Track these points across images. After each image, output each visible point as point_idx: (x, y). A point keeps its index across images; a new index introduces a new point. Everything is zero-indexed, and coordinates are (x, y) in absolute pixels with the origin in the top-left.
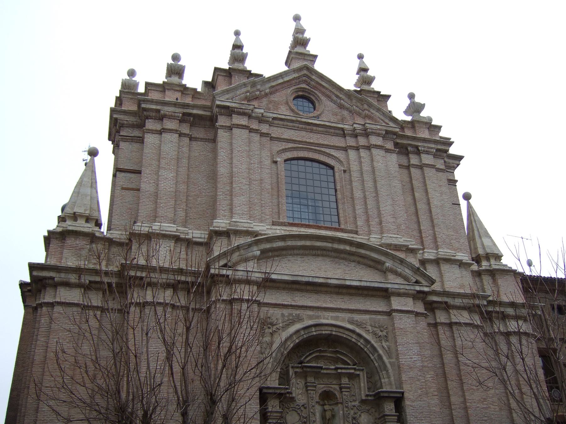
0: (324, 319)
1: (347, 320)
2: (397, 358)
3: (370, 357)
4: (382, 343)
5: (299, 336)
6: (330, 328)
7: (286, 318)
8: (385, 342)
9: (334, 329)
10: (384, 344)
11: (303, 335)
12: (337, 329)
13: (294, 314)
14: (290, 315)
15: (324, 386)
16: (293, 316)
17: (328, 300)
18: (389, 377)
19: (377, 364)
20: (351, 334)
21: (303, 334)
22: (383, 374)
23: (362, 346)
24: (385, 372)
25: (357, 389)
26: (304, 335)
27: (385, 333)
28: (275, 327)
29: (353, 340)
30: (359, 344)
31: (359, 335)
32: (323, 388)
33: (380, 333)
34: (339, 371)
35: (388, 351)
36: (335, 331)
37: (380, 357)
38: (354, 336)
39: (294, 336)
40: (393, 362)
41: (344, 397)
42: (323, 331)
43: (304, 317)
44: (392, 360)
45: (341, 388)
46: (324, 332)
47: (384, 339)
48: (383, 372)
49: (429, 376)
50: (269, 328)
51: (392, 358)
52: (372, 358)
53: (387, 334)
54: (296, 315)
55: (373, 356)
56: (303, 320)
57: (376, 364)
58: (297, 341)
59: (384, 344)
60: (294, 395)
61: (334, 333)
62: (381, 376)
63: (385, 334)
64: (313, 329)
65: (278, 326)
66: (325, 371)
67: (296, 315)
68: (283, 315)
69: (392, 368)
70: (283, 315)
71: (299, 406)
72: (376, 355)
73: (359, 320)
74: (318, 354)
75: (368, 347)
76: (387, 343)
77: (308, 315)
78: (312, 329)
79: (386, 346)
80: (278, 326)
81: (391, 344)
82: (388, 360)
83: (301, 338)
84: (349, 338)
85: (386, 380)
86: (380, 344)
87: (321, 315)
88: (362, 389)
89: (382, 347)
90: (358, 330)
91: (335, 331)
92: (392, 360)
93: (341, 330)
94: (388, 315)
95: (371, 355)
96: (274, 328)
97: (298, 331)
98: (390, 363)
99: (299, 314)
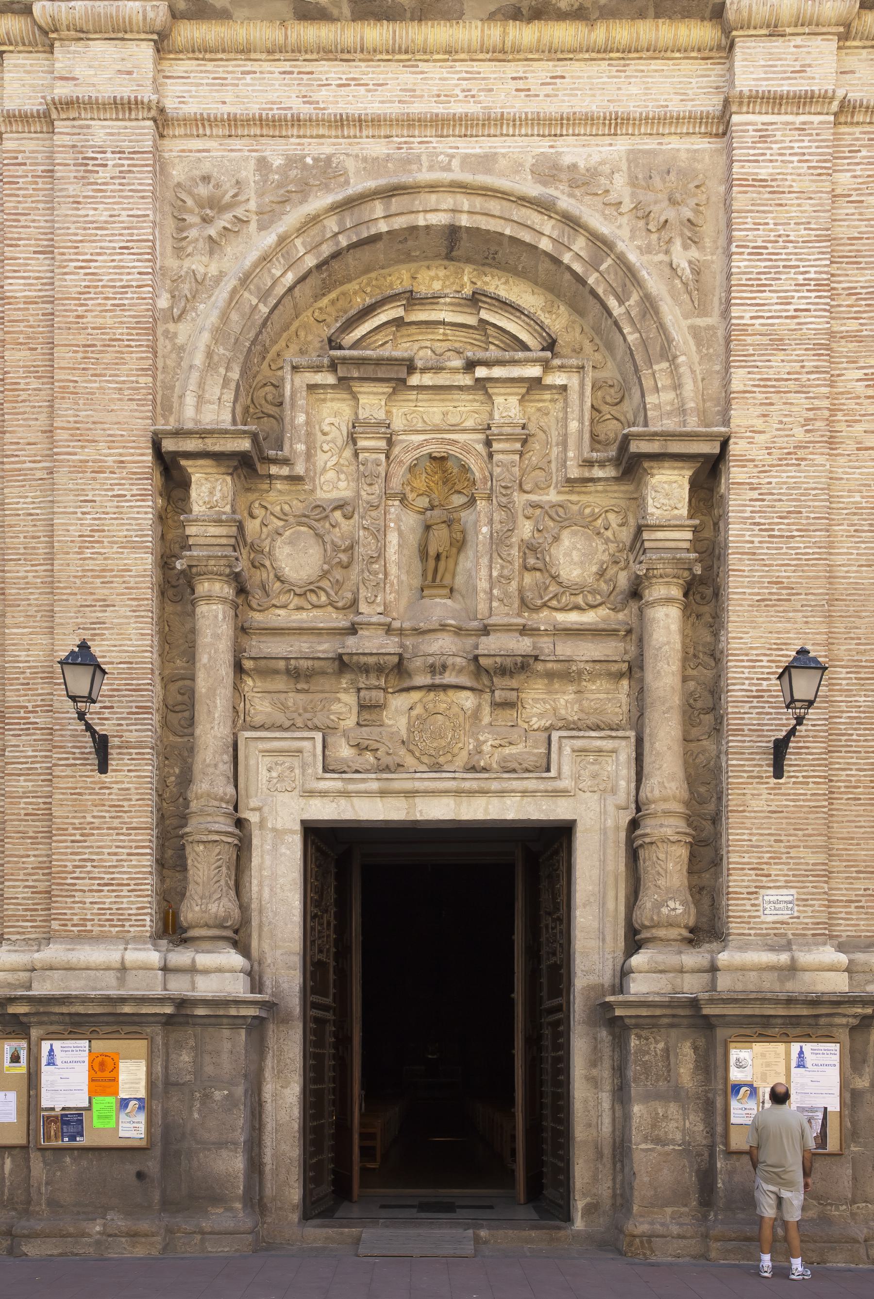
0: (431, 168)
1: (528, 166)
2: (726, 313)
3: (610, 314)
4: (667, 252)
5: (318, 239)
6: (448, 201)
7: (276, 177)
8: (685, 247)
9: (465, 203)
10: (681, 257)
11: (336, 235)
12: (479, 203)
13: (309, 160)
14: (292, 161)
15: (422, 437)
16: (305, 166)
17: (457, 91)
18: (677, 387)
19: (637, 335)
20: (535, 218)
21: (336, 229)
22: (654, 374)
23: (577, 267)
24: (665, 365)
25: (557, 445)
26: (340, 237)
27: (687, 213)
28: (228, 216)
29: (545, 244)
30: (566, 258)
31: (571, 222)
32: (420, 446)
33: (670, 214)
34: (481, 372)
35: (691, 286)
36: (469, 212)
37: (649, 305)
38: (548, 226)
39: (298, 242)
40: (708, 328)
41: (497, 470)
42: (421, 216)
43: (351, 165)
44: (701, 322)
45: (488, 443)
46: (421, 221)
47: (682, 235)
48: (656, 367)
49: (860, 374)
50: (206, 220)
51: (705, 315)
52: (617, 310)
53: (697, 212)
54: (314, 159)
55: (621, 302)
56: (342, 179)
57: (630, 338)
58: (310, 261)
59: (681, 257)
60: (300, 469)
61: (464, 221)
62: (648, 383)
63: (689, 214)
64: (378, 209)
65: (239, 212)
66: (427, 379)
67: (315, 160)
68: (263, 164)
69: (699, 351)
70: (263, 164)
71: (324, 509)
72: (634, 298)
73: (582, 165)
74: (399, 312)
75: (603, 268)
76: (694, 253)
77: (365, 160)
78: (373, 210)
79: (685, 265)
80: (239, 212)
81: (709, 258)
82: (689, 321)
83: (326, 250)
84: (526, 236)
85: (668, 396)
86: (661, 257)
87: (419, 156)
88: (572, 442)
89: (667, 270)
90: (565, 203)
91: (469, 212)
92: (701, 322)
93: (494, 206)
94: (717, 135)
95: (612, 303)
96: (224, 220)
97: (314, 220)
98: (696, 332)
99: (329, 159)
